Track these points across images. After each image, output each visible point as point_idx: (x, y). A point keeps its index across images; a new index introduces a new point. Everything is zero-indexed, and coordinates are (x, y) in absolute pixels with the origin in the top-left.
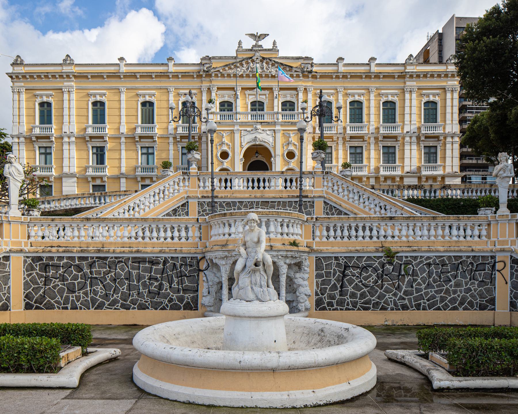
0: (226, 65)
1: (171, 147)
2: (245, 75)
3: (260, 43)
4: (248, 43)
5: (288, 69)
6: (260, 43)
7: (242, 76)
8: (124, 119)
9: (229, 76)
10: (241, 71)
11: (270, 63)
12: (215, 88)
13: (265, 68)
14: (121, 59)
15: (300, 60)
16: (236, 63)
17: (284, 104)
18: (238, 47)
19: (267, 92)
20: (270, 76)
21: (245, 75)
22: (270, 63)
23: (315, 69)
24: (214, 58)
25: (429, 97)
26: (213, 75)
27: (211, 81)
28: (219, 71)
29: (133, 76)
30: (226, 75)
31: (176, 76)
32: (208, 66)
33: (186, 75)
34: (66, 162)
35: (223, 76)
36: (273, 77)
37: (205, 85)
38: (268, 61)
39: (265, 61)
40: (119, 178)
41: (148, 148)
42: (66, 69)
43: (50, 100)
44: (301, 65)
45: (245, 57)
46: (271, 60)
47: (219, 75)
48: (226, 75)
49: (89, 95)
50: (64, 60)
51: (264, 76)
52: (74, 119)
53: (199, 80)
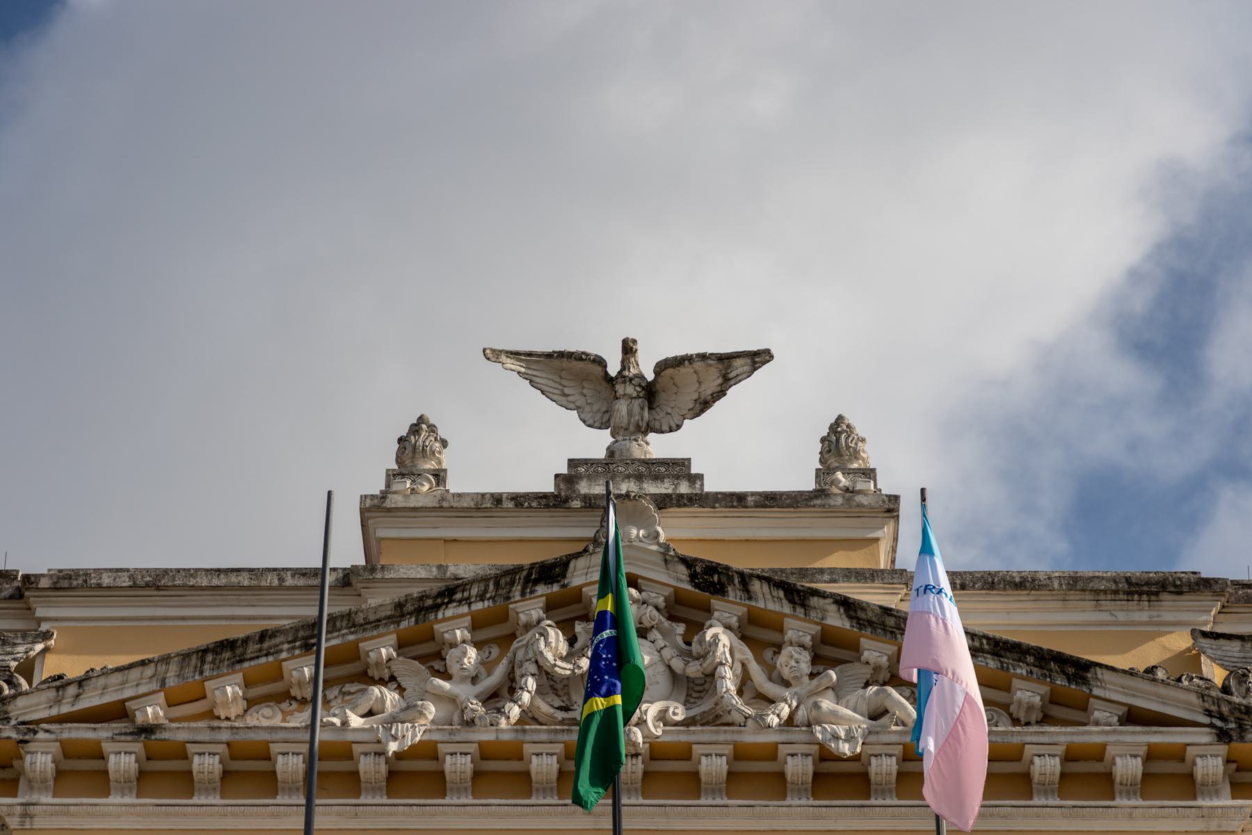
0: (227, 652)
2: (458, 765)
5: (1028, 693)
7: (416, 775)
9: (248, 771)
10: (409, 712)
11: (799, 629)
13: (728, 682)
15: (1170, 610)
16: (347, 621)
18: (391, 476)
20: (799, 767)
21: (458, 765)
22: (799, 629)
24: (69, 584)
26: (41, 760)
28: (117, 713)
30: (206, 764)
35: (165, 772)
36: (839, 778)
38: (768, 601)
39: (728, 608)
44: (1190, 661)
46: (798, 596)
47: (122, 762)
48: (206, 764)
51: (713, 766)
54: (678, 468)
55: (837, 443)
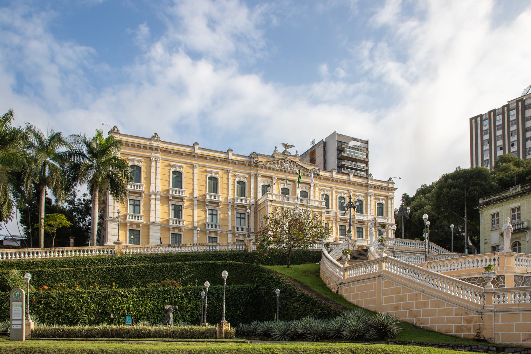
1: (230, 213)
3: (288, 150)
4: (281, 149)
6: (288, 150)
7: (278, 170)
8: (196, 187)
12: (260, 175)
14: (196, 144)
17: (302, 192)
19: (292, 183)
23: (321, 173)
25: (379, 200)
27: (257, 171)
29: (205, 158)
31: (234, 162)
32: (256, 159)
33: (241, 163)
34: (152, 214)
35: (266, 168)
37: (253, 172)
39: (292, 163)
40: (193, 230)
41: (212, 210)
42: (154, 144)
43: (140, 164)
45: (280, 158)
49: (170, 165)
50: (153, 137)
52: (159, 181)
53: (249, 168)
54: (289, 152)
55: (297, 152)
